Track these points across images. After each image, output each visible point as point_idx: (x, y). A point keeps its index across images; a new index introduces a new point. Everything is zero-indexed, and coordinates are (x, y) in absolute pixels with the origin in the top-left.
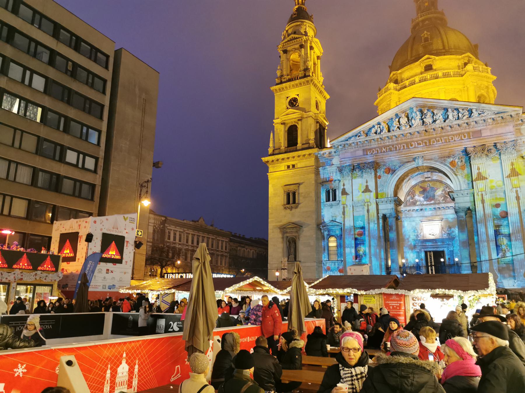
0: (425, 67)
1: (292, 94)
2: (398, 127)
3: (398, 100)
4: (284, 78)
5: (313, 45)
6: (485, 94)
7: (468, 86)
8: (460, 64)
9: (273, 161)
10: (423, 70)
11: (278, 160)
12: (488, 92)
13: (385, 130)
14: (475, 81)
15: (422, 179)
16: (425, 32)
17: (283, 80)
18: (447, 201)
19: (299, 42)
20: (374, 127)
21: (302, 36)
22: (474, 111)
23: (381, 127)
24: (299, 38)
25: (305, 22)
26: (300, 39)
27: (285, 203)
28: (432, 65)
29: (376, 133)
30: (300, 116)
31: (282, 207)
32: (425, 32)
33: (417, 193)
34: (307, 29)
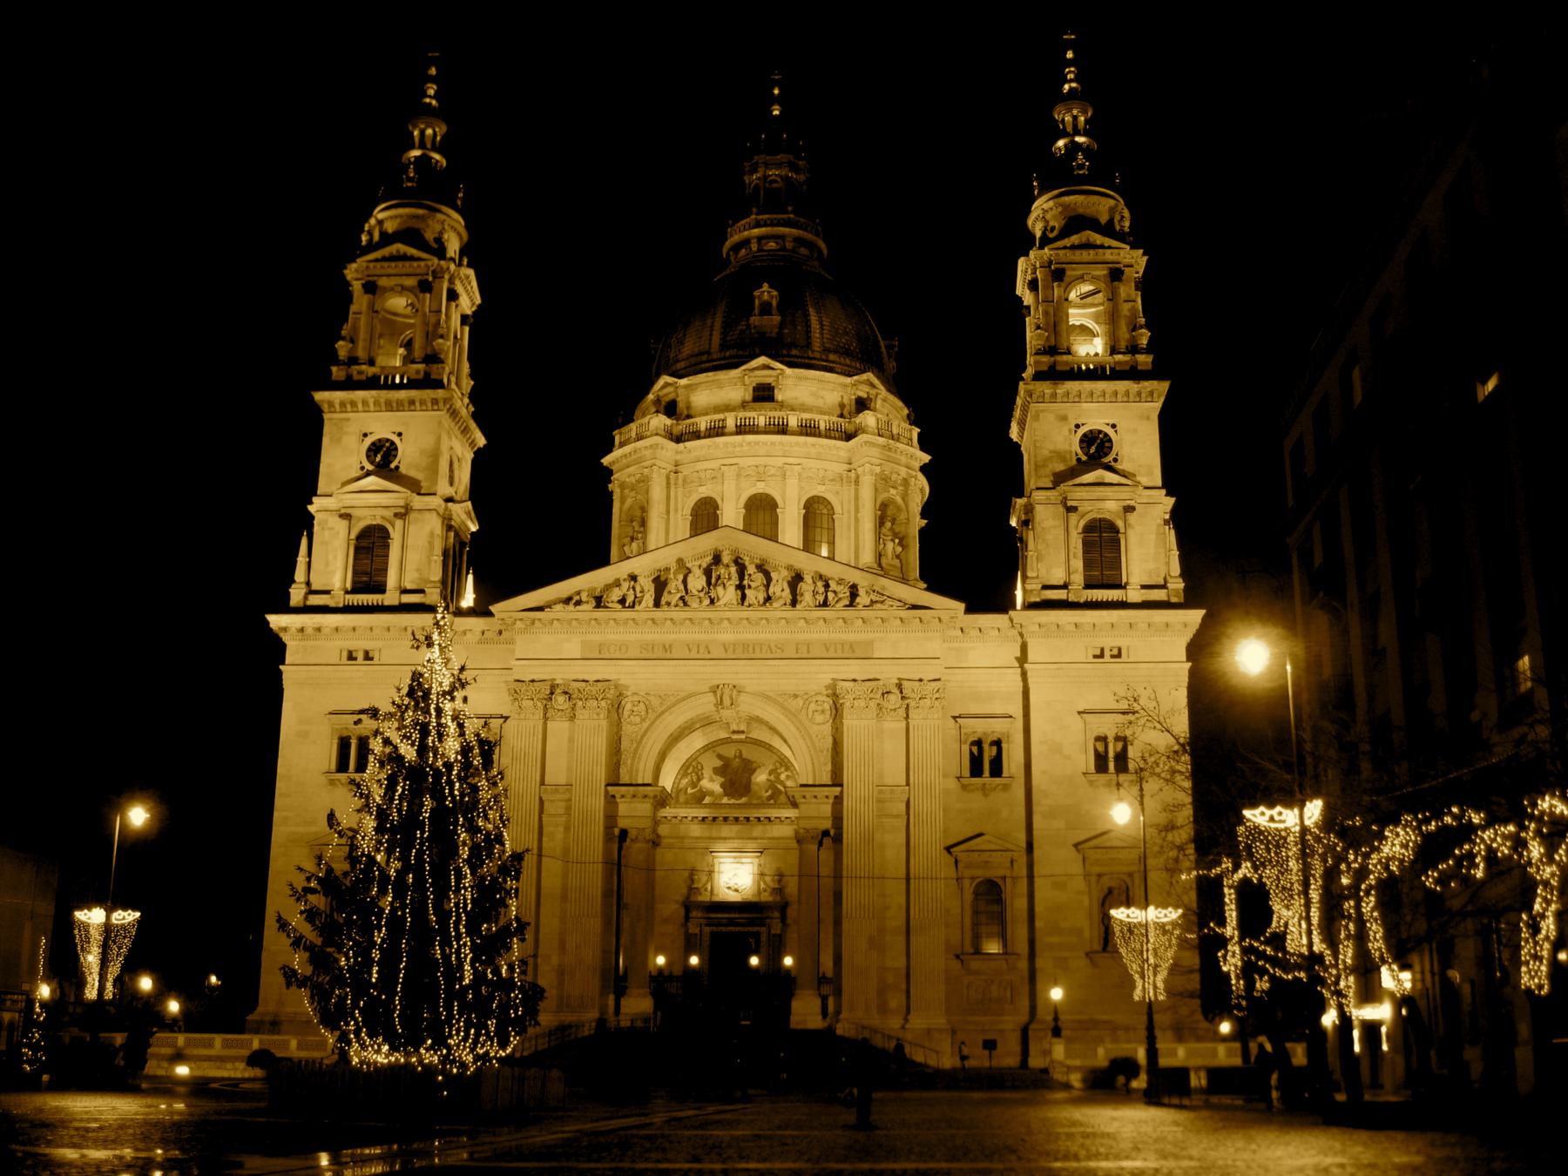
0: (755, 389)
1: (382, 426)
2: (682, 598)
3: (674, 468)
4: (360, 373)
5: (459, 288)
6: (899, 500)
7: (860, 470)
8: (846, 401)
9: (302, 630)
10: (749, 396)
11: (319, 630)
12: (905, 497)
13: (649, 599)
14: (878, 462)
15: (723, 735)
16: (766, 287)
17: (356, 377)
18: (779, 802)
19: (418, 271)
20: (617, 584)
21: (424, 255)
22: (862, 592)
23: (638, 589)
24: (419, 259)
25: (440, 211)
26: (422, 264)
27: (333, 767)
28: (773, 388)
29: (622, 601)
30: (402, 503)
31: (323, 779)
32: (766, 287)
33: (707, 772)
34: (446, 236)
